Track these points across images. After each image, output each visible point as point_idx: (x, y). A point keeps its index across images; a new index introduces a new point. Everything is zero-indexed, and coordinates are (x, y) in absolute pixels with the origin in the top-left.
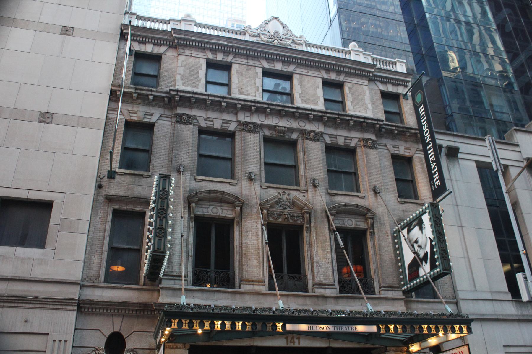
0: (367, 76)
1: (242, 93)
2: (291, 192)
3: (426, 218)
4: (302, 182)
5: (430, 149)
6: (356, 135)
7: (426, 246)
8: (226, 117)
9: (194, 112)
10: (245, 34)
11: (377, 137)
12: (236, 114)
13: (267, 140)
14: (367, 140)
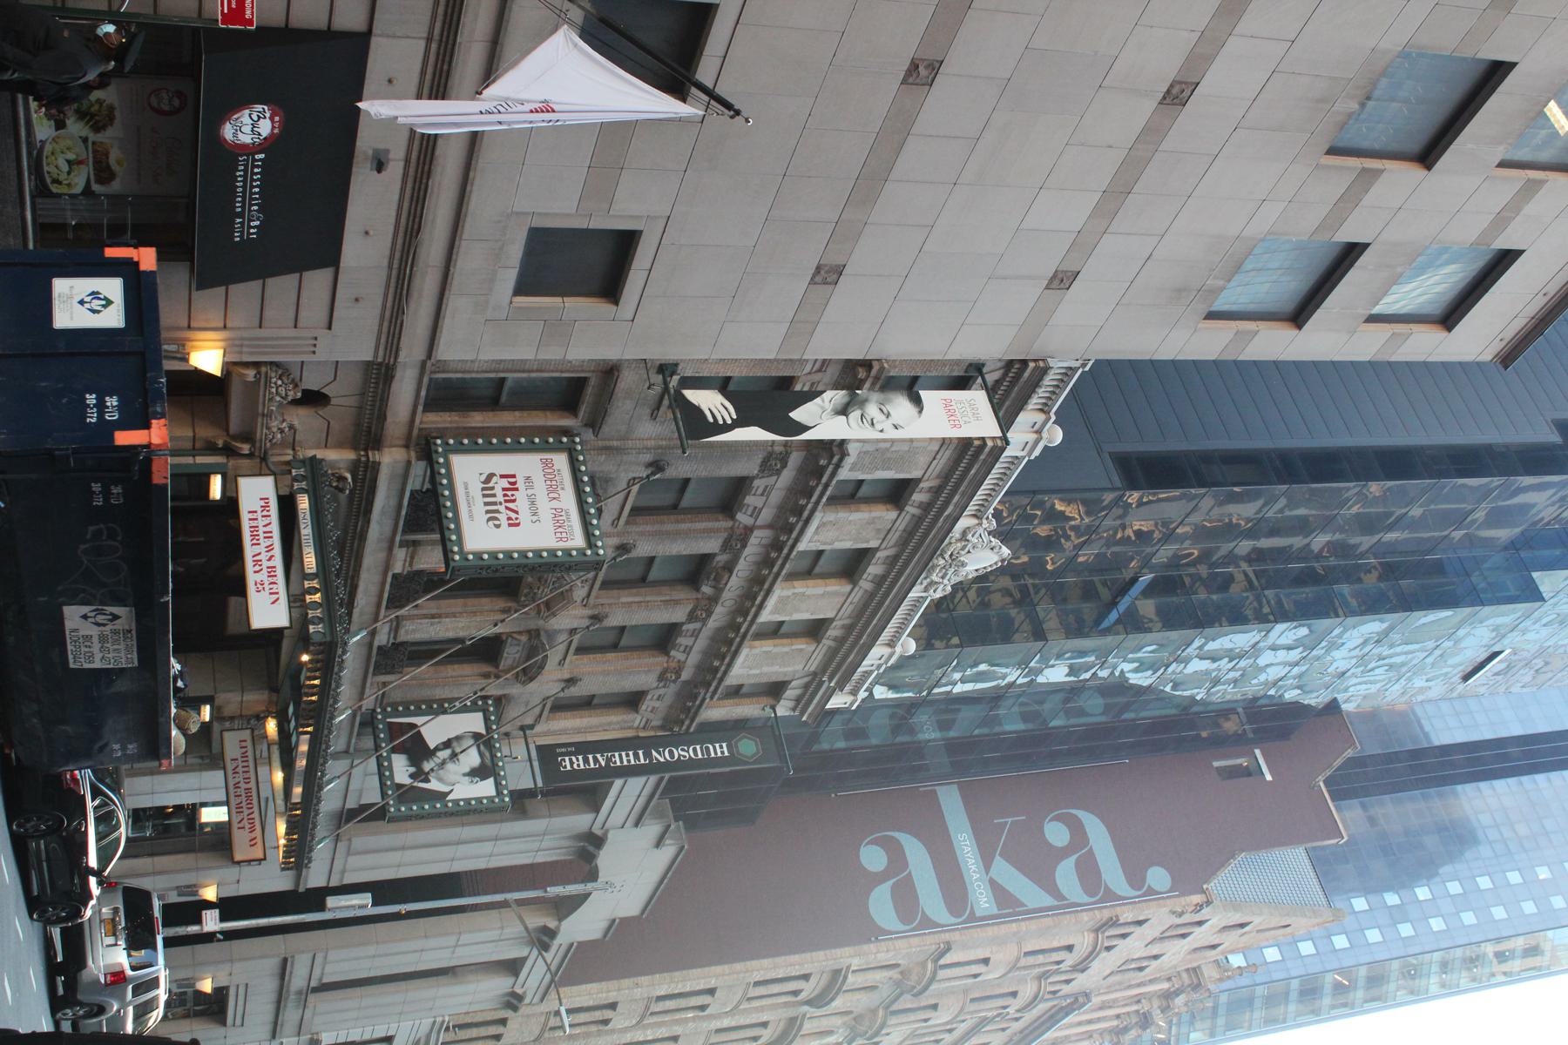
0: (824, 672)
1: (822, 525)
2: (586, 589)
3: (486, 788)
4: (607, 598)
5: (636, 756)
6: (694, 659)
7: (440, 780)
8: (766, 516)
9: (787, 475)
10: (974, 516)
11: (685, 682)
12: (770, 526)
13: (704, 560)
14: (678, 672)
